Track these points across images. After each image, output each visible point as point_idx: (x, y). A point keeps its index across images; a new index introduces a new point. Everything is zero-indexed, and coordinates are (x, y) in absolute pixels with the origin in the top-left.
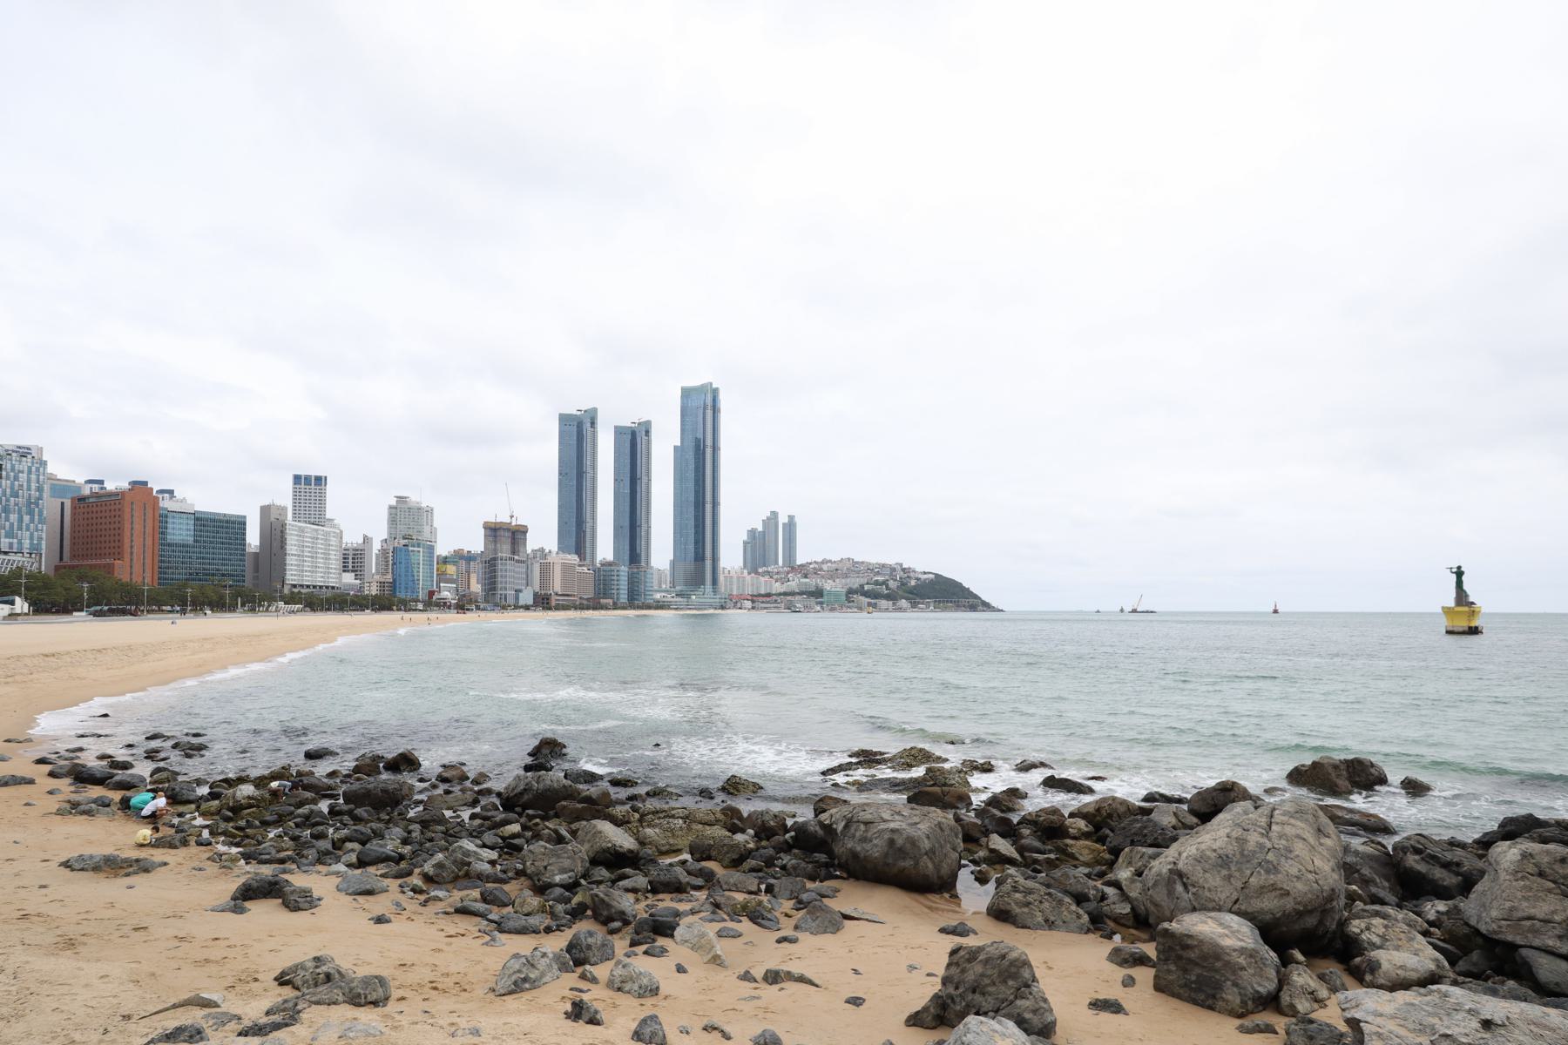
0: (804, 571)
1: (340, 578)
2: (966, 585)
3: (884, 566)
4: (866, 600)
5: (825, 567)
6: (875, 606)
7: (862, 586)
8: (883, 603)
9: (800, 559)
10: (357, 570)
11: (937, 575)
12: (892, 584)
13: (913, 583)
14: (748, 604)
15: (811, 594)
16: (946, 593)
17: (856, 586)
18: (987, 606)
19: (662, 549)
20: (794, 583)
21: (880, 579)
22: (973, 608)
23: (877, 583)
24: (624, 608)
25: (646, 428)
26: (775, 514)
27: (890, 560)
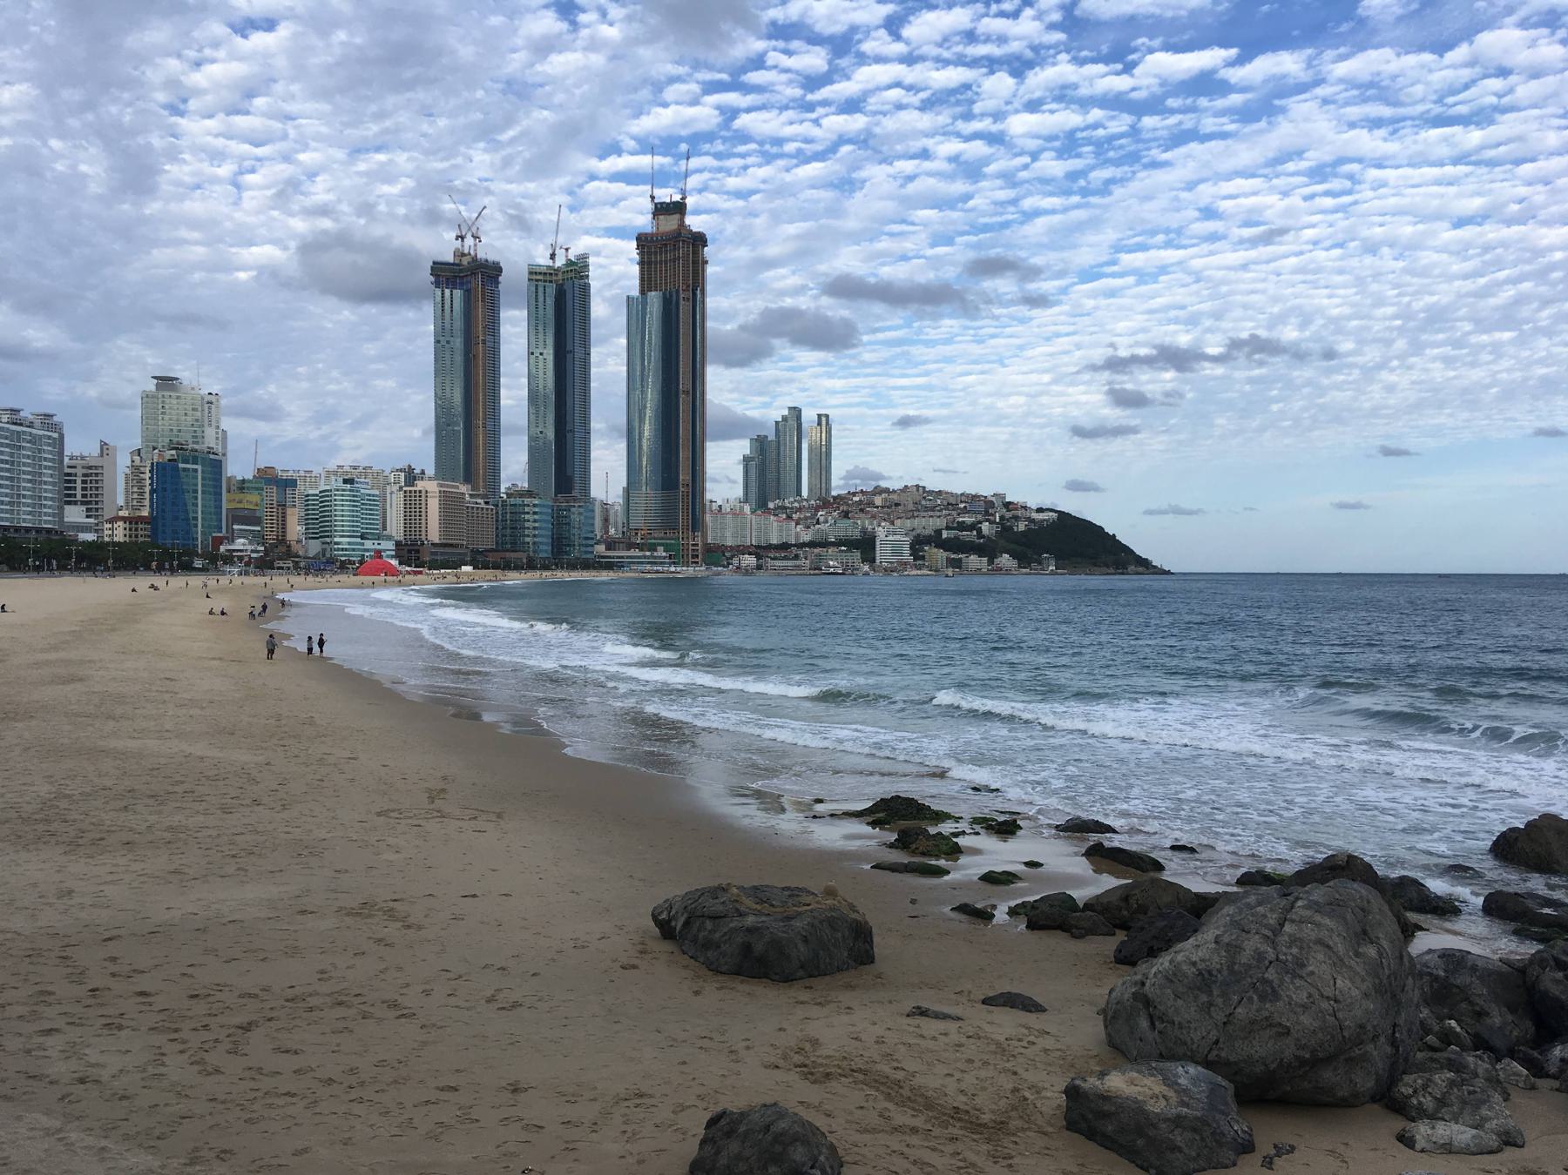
0: (843, 506)
1: (61, 515)
2: (1110, 530)
3: (975, 497)
4: (941, 555)
5: (878, 501)
6: (956, 564)
7: (939, 532)
8: (974, 561)
9: (838, 486)
10: (92, 504)
12: (985, 527)
13: (1022, 527)
14: (749, 560)
15: (851, 544)
17: (929, 532)
18: (1144, 563)
19: (608, 470)
20: (830, 525)
21: (968, 519)
23: (962, 527)
24: (546, 568)
26: (796, 412)
27: (986, 491)
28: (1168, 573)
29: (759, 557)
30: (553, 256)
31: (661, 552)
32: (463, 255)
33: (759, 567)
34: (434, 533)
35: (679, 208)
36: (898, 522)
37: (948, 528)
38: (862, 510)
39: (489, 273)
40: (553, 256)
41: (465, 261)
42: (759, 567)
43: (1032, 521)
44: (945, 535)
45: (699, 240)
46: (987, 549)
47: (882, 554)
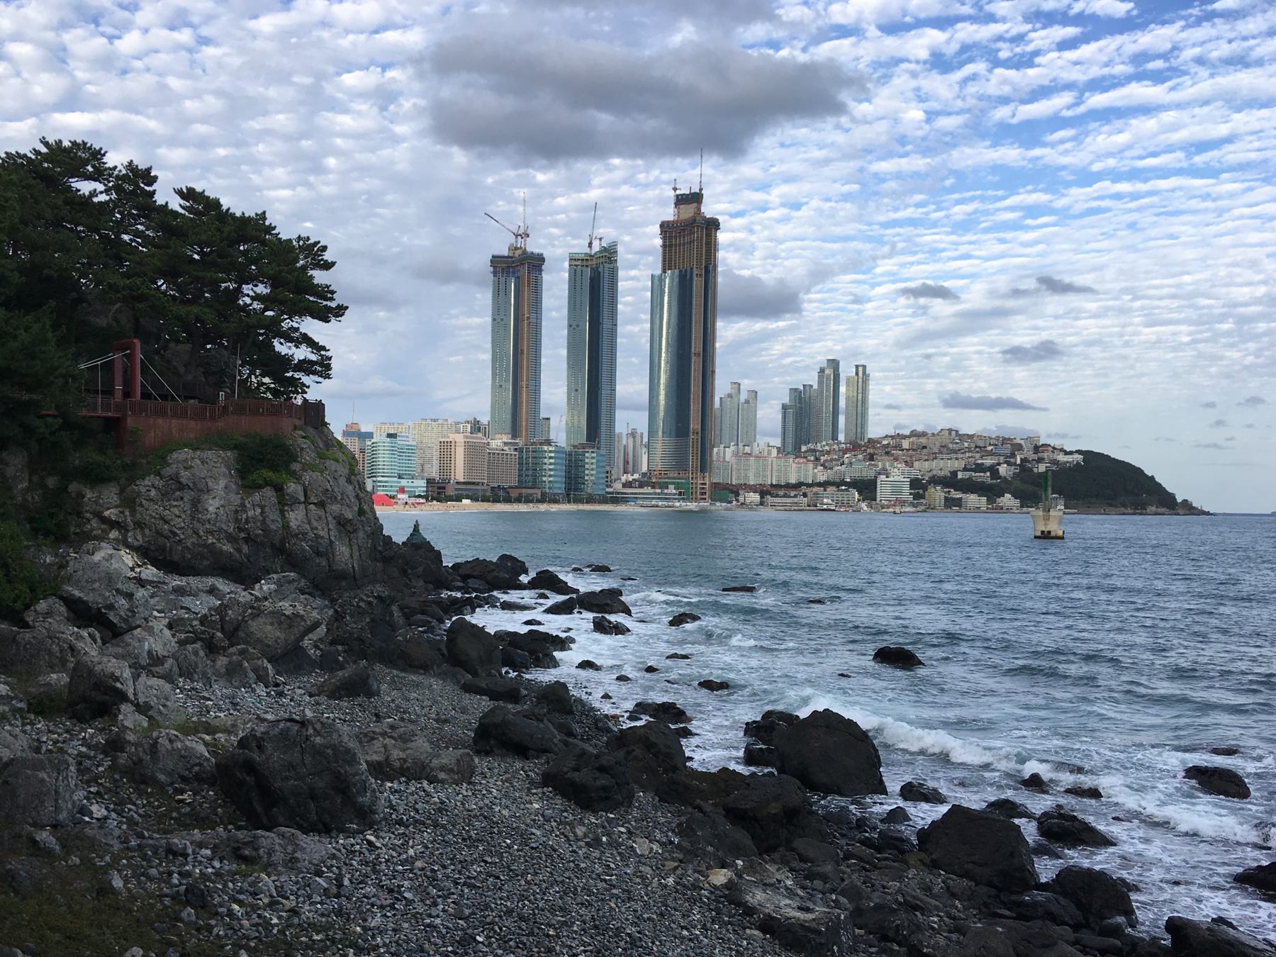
4: (937, 494)
7: (954, 473)
8: (972, 499)
11: (1088, 455)
12: (1003, 470)
13: (1042, 468)
14: (754, 497)
16: (1107, 484)
17: (946, 473)
21: (988, 461)
22: (1139, 507)
23: (980, 468)
25: (609, 254)
28: (1208, 513)
29: (763, 494)
30: (590, 245)
31: (672, 490)
32: (516, 249)
33: (762, 503)
34: (459, 474)
35: (696, 198)
36: (916, 464)
37: (965, 469)
38: (887, 453)
39: (536, 263)
40: (590, 245)
41: (518, 253)
42: (762, 503)
43: (1055, 462)
44: (960, 475)
45: (713, 225)
46: (992, 491)
47: (883, 492)
